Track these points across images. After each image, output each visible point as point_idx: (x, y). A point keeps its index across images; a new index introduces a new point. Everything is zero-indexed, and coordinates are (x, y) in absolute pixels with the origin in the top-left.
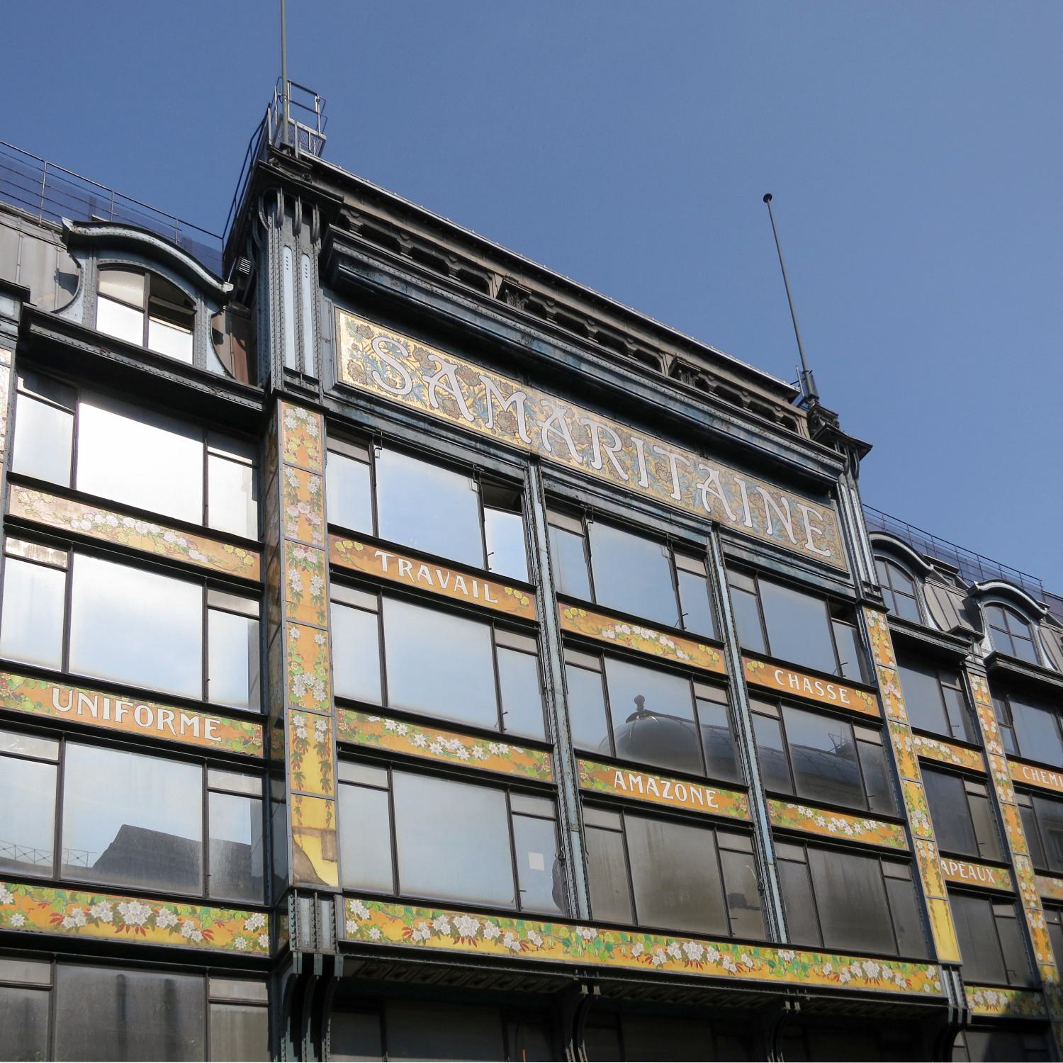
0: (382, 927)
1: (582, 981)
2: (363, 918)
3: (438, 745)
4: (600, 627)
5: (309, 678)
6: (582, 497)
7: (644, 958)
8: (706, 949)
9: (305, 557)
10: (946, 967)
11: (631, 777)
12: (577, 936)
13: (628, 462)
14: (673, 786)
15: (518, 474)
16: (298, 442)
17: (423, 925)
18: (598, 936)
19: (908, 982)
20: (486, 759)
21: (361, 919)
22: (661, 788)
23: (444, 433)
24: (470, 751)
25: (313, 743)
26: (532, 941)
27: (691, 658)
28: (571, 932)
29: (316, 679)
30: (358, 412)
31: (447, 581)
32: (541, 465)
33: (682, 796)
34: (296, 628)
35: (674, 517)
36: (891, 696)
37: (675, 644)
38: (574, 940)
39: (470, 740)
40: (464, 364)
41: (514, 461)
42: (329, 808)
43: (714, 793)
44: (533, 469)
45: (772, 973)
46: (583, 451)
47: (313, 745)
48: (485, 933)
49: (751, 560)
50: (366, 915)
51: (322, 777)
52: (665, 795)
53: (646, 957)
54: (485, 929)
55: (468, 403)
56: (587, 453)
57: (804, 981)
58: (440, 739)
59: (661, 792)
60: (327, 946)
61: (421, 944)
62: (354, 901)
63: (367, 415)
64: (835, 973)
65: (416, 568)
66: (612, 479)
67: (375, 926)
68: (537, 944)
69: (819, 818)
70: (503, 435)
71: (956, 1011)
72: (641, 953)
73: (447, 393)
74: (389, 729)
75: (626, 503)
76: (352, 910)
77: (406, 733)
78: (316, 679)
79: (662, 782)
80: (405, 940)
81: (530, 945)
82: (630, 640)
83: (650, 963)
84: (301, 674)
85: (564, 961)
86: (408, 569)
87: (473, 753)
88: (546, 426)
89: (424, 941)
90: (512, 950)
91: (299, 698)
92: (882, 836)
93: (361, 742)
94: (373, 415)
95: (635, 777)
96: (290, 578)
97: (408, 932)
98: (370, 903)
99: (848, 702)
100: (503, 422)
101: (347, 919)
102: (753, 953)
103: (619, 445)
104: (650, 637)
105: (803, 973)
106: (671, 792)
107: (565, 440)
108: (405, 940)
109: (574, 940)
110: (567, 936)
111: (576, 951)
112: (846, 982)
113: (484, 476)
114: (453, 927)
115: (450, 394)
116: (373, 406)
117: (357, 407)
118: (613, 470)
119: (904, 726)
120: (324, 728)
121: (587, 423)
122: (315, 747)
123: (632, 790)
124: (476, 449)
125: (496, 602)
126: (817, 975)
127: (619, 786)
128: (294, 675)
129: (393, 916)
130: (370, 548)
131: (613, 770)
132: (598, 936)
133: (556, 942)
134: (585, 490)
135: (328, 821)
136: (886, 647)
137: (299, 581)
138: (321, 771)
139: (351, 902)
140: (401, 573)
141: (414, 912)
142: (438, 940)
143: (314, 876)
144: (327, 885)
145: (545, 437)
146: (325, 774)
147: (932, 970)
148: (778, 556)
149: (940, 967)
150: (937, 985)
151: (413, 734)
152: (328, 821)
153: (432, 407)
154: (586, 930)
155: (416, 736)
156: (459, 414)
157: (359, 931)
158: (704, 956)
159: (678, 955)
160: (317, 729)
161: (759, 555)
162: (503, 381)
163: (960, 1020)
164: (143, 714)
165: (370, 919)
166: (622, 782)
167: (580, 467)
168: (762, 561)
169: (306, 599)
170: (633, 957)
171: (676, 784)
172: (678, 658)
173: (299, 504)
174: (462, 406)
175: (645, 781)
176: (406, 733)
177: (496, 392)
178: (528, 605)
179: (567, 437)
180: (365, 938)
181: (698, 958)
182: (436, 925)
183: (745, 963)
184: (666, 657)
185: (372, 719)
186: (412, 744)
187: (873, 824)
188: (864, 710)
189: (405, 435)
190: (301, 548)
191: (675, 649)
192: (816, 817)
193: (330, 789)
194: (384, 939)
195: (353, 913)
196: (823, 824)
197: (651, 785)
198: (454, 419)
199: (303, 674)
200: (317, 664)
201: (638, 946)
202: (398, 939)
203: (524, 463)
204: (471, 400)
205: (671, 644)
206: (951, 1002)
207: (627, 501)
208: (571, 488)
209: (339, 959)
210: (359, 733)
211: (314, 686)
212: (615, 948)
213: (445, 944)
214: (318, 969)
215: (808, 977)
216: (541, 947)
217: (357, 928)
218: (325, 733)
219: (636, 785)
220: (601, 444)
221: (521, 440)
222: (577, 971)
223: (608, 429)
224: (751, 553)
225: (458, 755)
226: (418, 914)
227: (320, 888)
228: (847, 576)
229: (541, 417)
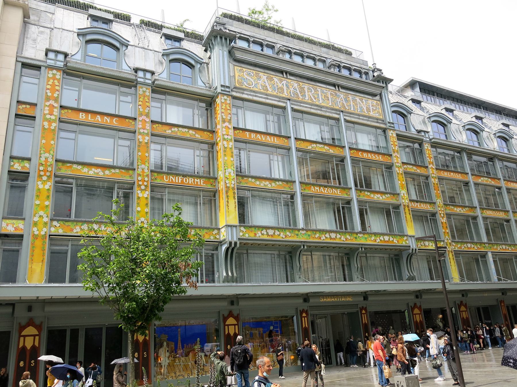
10: (410, 236)
11: (316, 188)
12: (300, 233)
13: (316, 96)
14: (328, 189)
15: (284, 105)
17: (259, 232)
19: (398, 241)
22: (324, 190)
33: (330, 192)
44: (288, 102)
46: (302, 95)
50: (244, 230)
52: (325, 192)
55: (270, 86)
56: (304, 96)
58: (263, 182)
59: (324, 191)
60: (235, 239)
71: (413, 249)
81: (287, 236)
88: (292, 89)
100: (280, 90)
103: (313, 92)
114: (267, 232)
118: (311, 100)
145: (292, 93)
147: (405, 238)
150: (407, 242)
156: (268, 90)
158: (336, 237)
159: (328, 237)
163: (414, 252)
164: (186, 179)
166: (313, 189)
174: (268, 87)
175: (320, 189)
177: (278, 82)
179: (298, 92)
181: (334, 237)
182: (262, 232)
206: (411, 247)
209: (238, 243)
213: (265, 237)
214: (233, 246)
220: (308, 92)
221: (285, 95)
229: (291, 87)
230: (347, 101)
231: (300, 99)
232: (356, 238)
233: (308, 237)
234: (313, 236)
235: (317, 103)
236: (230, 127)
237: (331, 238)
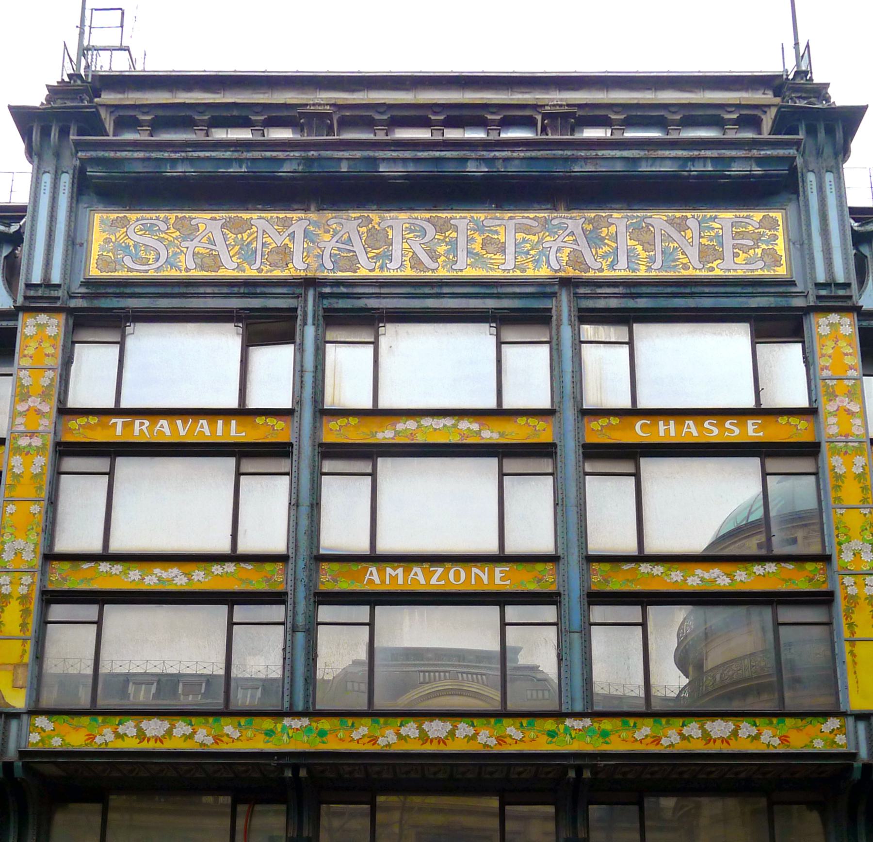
0: (64, 736)
1: (281, 768)
2: (47, 730)
3: (155, 576)
4: (374, 430)
5: (20, 543)
6: (373, 303)
7: (367, 740)
8: (456, 726)
9: (30, 443)
16: (37, 345)
18: (310, 725)
20: (207, 580)
21: (44, 731)
23: (202, 290)
24: (190, 576)
25: (16, 595)
26: (227, 735)
27: (502, 435)
28: (276, 723)
29: (27, 543)
30: (108, 300)
31: (187, 429)
32: (319, 286)
34: (13, 505)
35: (500, 290)
36: (841, 410)
37: (481, 425)
38: (279, 730)
39: (189, 567)
40: (233, 215)
41: (286, 292)
42: (25, 646)
43: (508, 569)
45: (550, 743)
47: (15, 599)
48: (174, 732)
49: (623, 306)
51: (21, 621)
53: (369, 739)
54: (175, 728)
57: (600, 748)
61: (103, 746)
62: (40, 717)
63: (118, 299)
64: (654, 737)
65: (153, 424)
66: (415, 274)
67: (58, 735)
68: (233, 737)
69: (672, 573)
70: (271, 271)
72: (364, 736)
73: (208, 250)
74: (103, 571)
75: (434, 294)
76: (36, 725)
77: (120, 572)
78: (27, 543)
79: (431, 569)
80: (86, 745)
82: (415, 435)
83: (373, 744)
84: (12, 542)
85: (262, 750)
86: (144, 427)
87: (193, 577)
89: (106, 744)
90: (203, 744)
91: (8, 561)
92: (783, 580)
93: (71, 587)
94: (122, 297)
95: (395, 569)
96: (13, 464)
97: (91, 737)
98: (55, 718)
99: (761, 434)
100: (275, 258)
101: (30, 732)
102: (524, 725)
104: (445, 426)
105: (601, 740)
106: (457, 575)
107: (355, 252)
108: (86, 745)
109: (279, 730)
110: (272, 726)
111: (280, 740)
112: (672, 745)
113: (249, 317)
115: (212, 250)
116: (122, 290)
117: (105, 295)
118: (416, 262)
119: (856, 444)
120: (30, 581)
121: (389, 224)
122: (17, 600)
123: (388, 582)
124: (241, 294)
125: (244, 434)
126: (624, 740)
127: (371, 581)
128: (6, 543)
129: (76, 726)
130: (104, 419)
131: (364, 567)
132: (310, 725)
133: (257, 733)
134: (378, 296)
135: (22, 656)
136: (846, 354)
137: (21, 464)
138: (21, 617)
139: (37, 719)
140: (137, 433)
141: (100, 721)
142: (122, 742)
143: (2, 702)
144: (14, 707)
146: (24, 620)
147: (834, 723)
148: (669, 290)
149: (851, 720)
151: (127, 571)
152: (22, 656)
153: (187, 270)
154: (296, 720)
155: (130, 572)
157: (42, 740)
160: (22, 584)
161: (636, 297)
162: (281, 215)
165: (53, 730)
167: (371, 274)
168: (642, 303)
169: (25, 480)
170: (352, 740)
171: (451, 568)
172: (483, 438)
173: (29, 399)
175: (407, 571)
176: (120, 572)
178: (282, 429)
180: (46, 746)
183: (510, 736)
184: (464, 441)
185: (86, 566)
186: (126, 580)
187: (771, 567)
188: (789, 438)
189: (158, 305)
190: (26, 436)
191: (480, 431)
192: (669, 572)
193: (28, 630)
194: (65, 745)
195: (37, 727)
196: (680, 579)
197: (416, 574)
198: (214, 274)
199: (15, 541)
200: (29, 530)
201: (360, 730)
202: (79, 744)
203: (298, 291)
204: (237, 248)
205: (475, 427)
207: (436, 290)
208: (360, 298)
210: (70, 580)
211: (23, 549)
212: (330, 733)
213: (131, 744)
215: (607, 743)
216: (238, 739)
217: (40, 738)
218: (29, 585)
219: (394, 578)
222: (276, 757)
223: (417, 222)
224: (625, 297)
225: (174, 582)
226: (103, 722)
227: (7, 710)
228: (792, 283)
229: (327, 237)
230: (594, 239)
231: (363, 273)
232: (552, 734)
233: (318, 740)
234: (341, 734)
235: (443, 273)
236: (45, 408)
237: (424, 737)
